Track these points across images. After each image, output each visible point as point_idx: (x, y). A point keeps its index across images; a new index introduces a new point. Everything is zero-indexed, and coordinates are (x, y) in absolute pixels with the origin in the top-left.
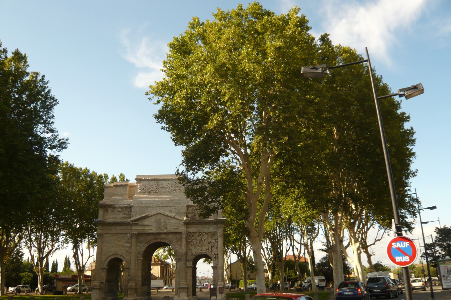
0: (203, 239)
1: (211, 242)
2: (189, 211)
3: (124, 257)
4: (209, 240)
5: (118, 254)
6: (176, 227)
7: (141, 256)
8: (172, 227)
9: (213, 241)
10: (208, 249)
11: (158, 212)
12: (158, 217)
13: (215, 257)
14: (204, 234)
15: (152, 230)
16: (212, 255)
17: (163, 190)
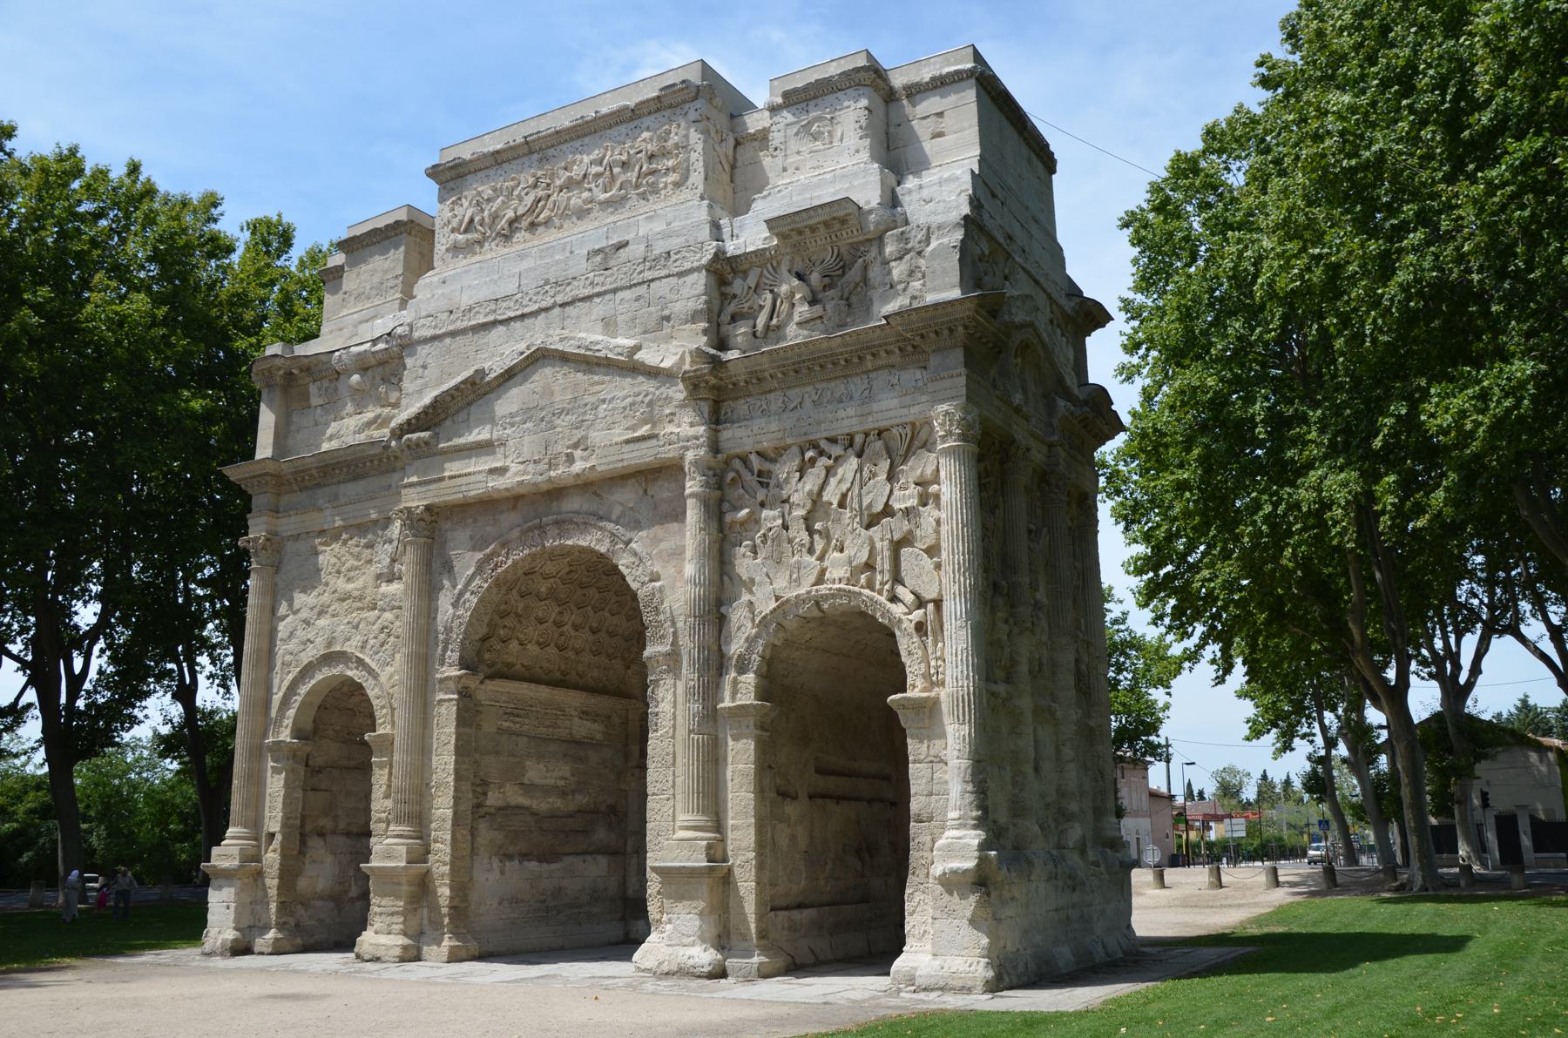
0: (831, 495)
1: (888, 511)
2: (731, 308)
3: (371, 671)
4: (875, 495)
5: (342, 657)
6: (644, 430)
7: (456, 656)
8: (619, 434)
9: (905, 498)
10: (869, 566)
11: (538, 341)
12: (546, 375)
13: (920, 627)
14: (836, 450)
15: (501, 471)
16: (898, 610)
17: (576, 199)
